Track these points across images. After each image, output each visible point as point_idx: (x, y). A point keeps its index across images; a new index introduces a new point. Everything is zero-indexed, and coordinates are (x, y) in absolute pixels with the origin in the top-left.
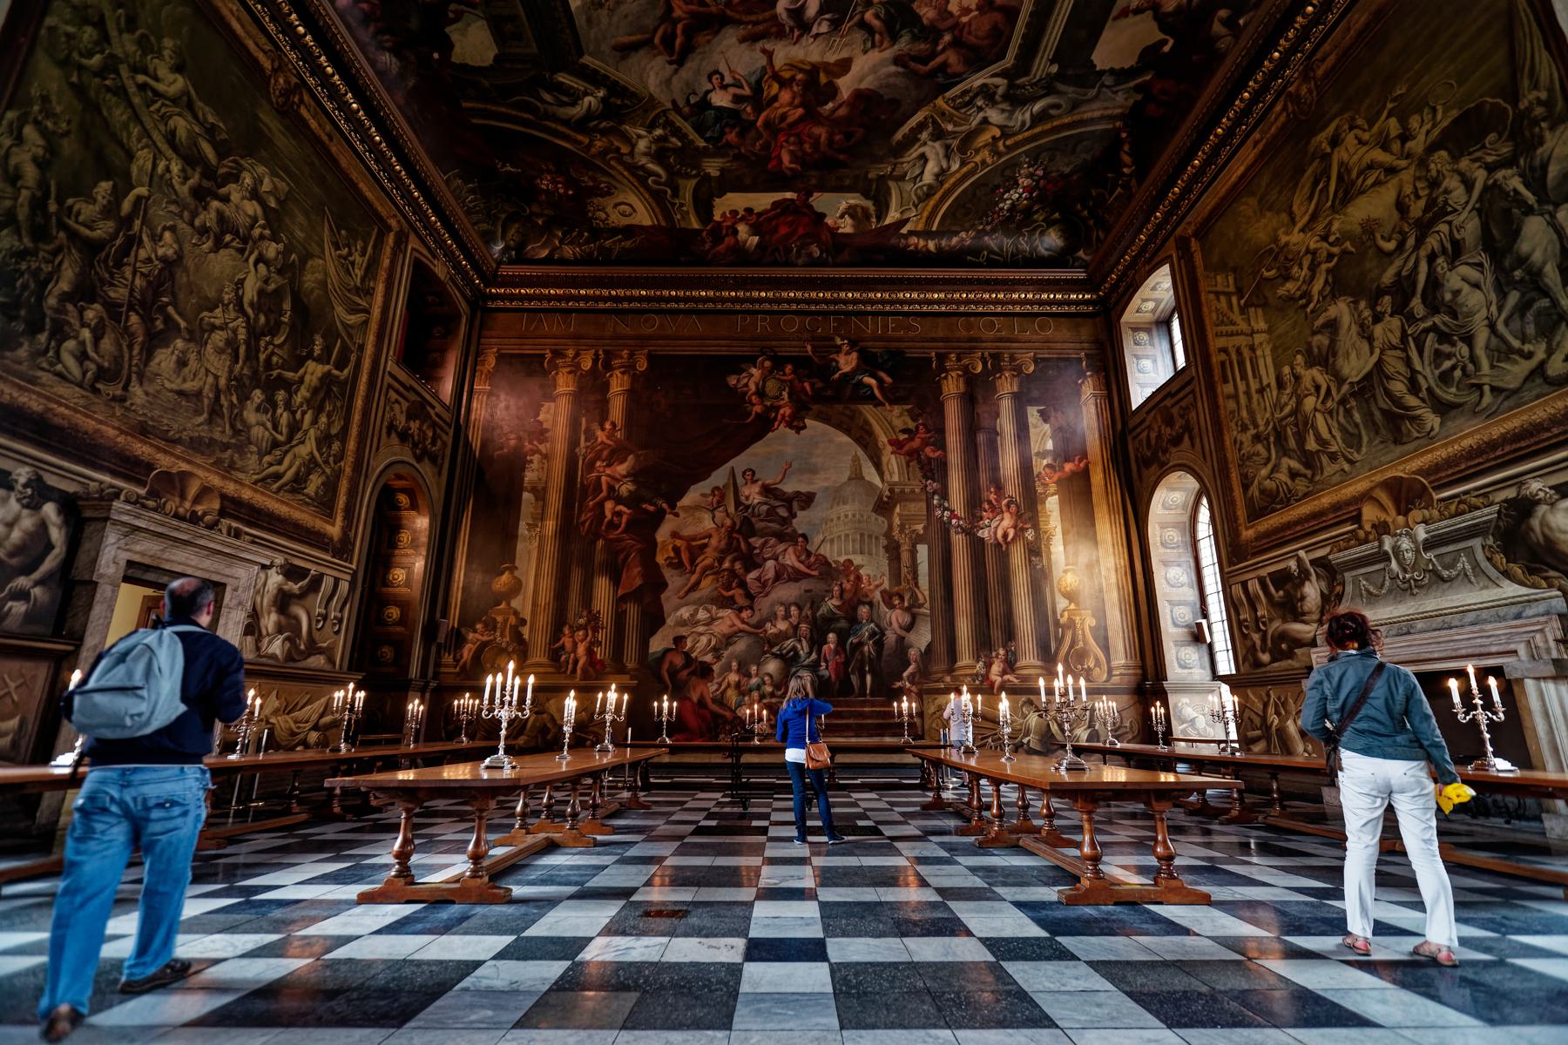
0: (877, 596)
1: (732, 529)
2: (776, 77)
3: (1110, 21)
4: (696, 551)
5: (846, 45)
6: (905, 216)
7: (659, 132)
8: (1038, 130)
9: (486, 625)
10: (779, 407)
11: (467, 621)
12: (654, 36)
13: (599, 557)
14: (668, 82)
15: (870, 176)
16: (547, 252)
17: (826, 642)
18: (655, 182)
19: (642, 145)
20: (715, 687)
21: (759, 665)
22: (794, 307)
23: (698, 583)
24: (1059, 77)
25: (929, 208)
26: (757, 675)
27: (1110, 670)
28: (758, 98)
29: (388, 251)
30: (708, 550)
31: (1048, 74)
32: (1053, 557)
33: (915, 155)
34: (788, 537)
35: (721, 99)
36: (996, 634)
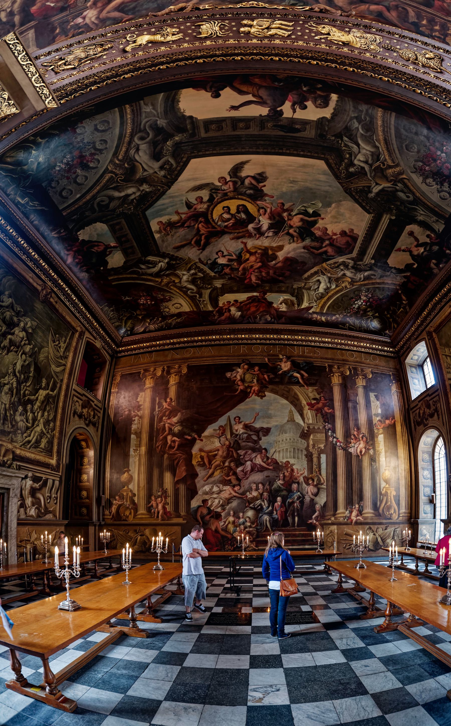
7: (192, 271)
9: (120, 497)
10: (252, 387)
11: (112, 496)
16: (143, 329)
20: (223, 523)
21: (243, 513)
22: (259, 341)
28: (239, 259)
29: (75, 340)
35: (222, 261)
36: (355, 498)
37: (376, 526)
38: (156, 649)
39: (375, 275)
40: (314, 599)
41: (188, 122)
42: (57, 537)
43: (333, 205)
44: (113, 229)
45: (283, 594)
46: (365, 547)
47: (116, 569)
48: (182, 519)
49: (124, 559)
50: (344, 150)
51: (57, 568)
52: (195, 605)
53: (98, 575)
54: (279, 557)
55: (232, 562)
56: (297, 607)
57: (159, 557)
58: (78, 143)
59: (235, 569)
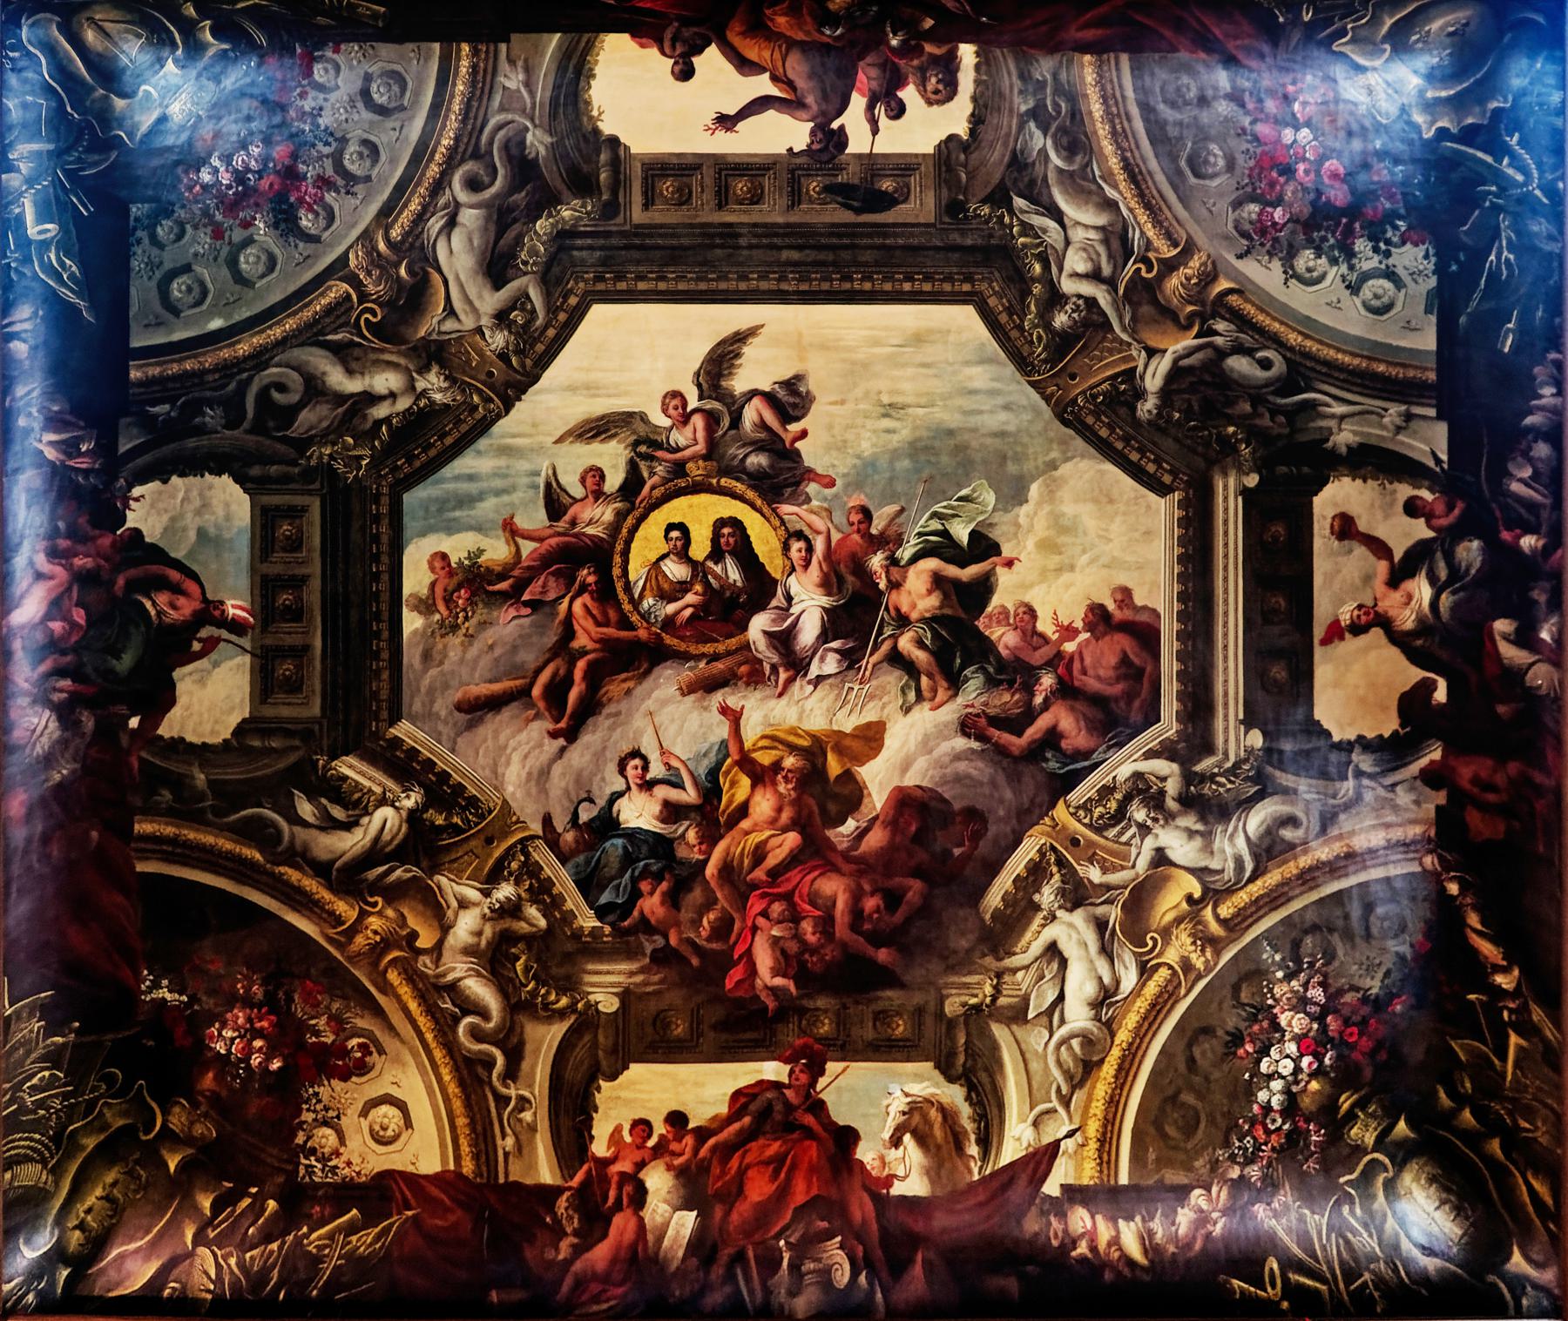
2: (746, 763)
3: (1318, 651)
5: (871, 697)
6: (1047, 1139)
7: (505, 891)
8: (1272, 878)
12: (532, 684)
14: (544, 774)
15: (947, 1010)
18: (476, 1034)
19: (465, 926)
24: (1268, 751)
25: (1098, 1108)
31: (1250, 751)
33: (1037, 947)
35: (639, 813)
39: (1292, 821)
41: (604, 157)
43: (1035, 490)
44: (265, 521)
50: (1024, 246)
58: (303, 115)
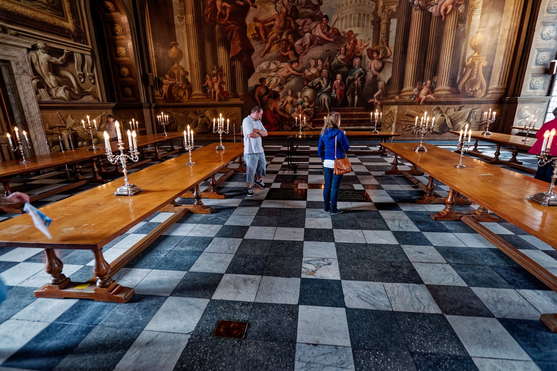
0: (365, 52)
1: (286, 15)
4: (268, 29)
9: (170, 76)
11: (161, 74)
13: (218, 36)
17: (336, 79)
20: (281, 103)
21: (301, 92)
23: (270, 48)
26: (301, 97)
27: (487, 91)
30: (274, 28)
32: (472, 23)
34: (318, 18)
36: (428, 72)
37: (446, 107)
38: (220, 224)
40: (367, 179)
42: (105, 121)
45: (337, 172)
46: (429, 129)
47: (178, 151)
48: (240, 99)
49: (186, 141)
51: (109, 153)
52: (255, 181)
53: (159, 158)
54: (334, 137)
55: (289, 142)
56: (349, 185)
57: (221, 138)
59: (292, 148)
